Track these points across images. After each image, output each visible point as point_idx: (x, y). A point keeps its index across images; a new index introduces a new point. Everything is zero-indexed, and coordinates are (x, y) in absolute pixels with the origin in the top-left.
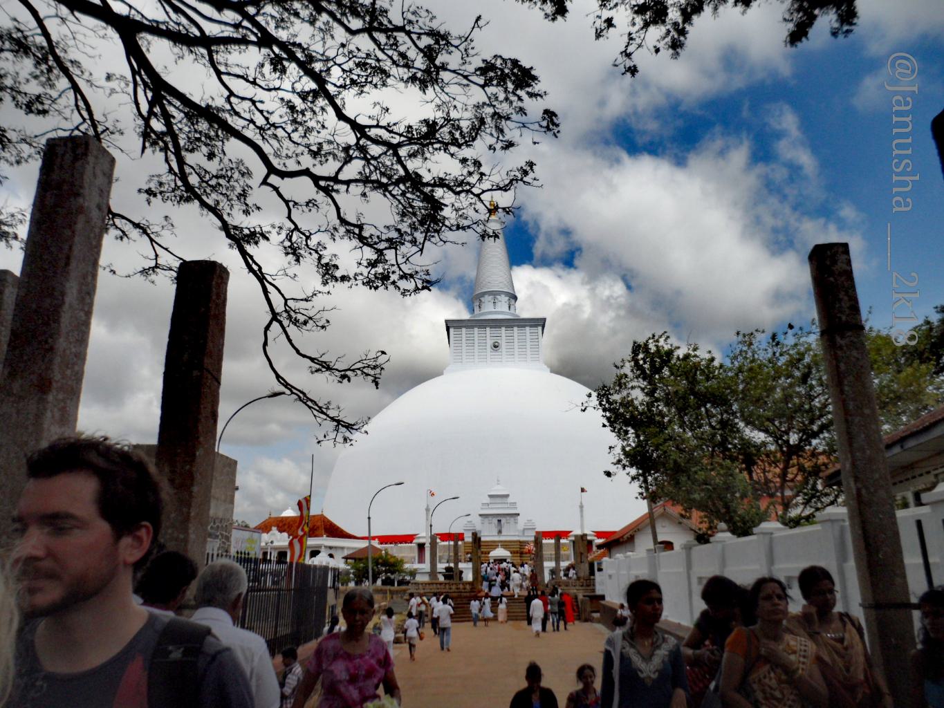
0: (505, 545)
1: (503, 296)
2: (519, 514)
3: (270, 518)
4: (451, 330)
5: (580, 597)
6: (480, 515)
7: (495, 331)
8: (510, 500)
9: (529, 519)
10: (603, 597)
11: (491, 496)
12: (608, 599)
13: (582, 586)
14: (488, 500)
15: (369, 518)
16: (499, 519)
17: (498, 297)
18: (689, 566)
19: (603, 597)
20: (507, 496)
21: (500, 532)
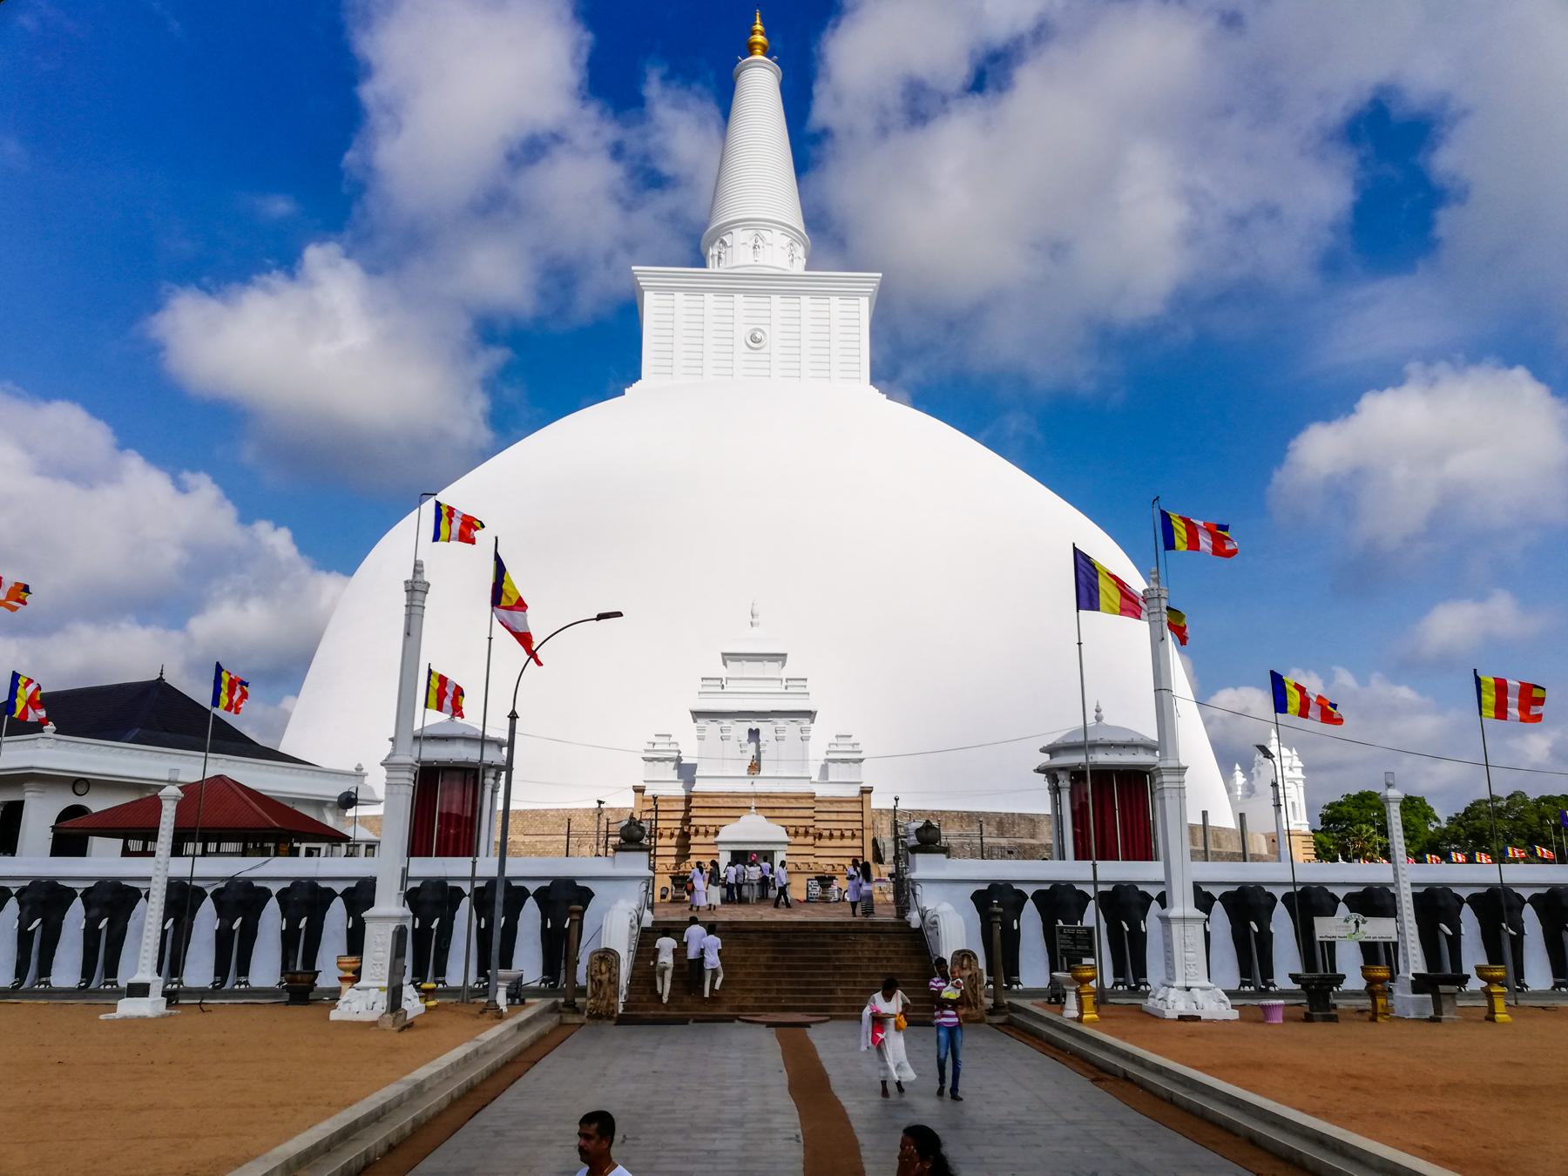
0: (770, 805)
2: (810, 714)
6: (697, 715)
7: (758, 302)
11: (728, 657)
20: (781, 658)
21: (755, 767)
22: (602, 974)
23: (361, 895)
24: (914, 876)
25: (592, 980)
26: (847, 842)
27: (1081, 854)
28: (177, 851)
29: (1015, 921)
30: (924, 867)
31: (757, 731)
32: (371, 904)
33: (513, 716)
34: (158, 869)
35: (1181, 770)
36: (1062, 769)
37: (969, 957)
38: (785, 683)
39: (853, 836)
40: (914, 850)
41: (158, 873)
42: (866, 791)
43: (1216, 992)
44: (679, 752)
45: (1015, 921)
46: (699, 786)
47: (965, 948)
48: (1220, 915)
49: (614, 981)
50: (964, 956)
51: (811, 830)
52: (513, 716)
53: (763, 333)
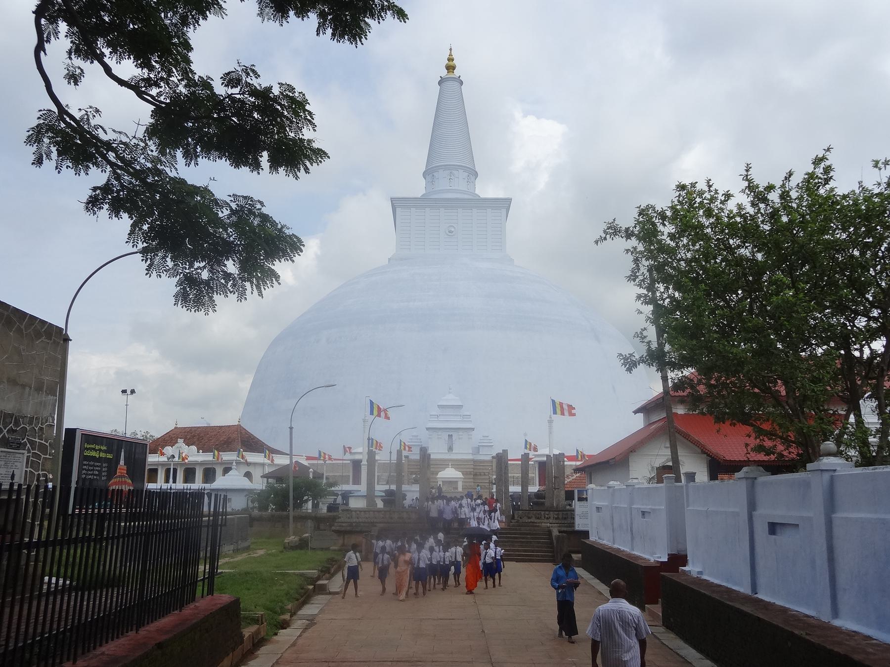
0: (458, 464)
2: (473, 429)
3: (176, 428)
4: (398, 210)
5: (555, 532)
6: (428, 429)
10: (586, 534)
12: (593, 538)
13: (556, 519)
15: (291, 428)
16: (451, 434)
17: (455, 172)
18: (752, 506)
19: (586, 534)
20: (460, 407)
21: (450, 449)
26: (483, 477)
31: (452, 435)
36: (536, 461)
44: (421, 442)
51: (472, 473)
53: (454, 228)
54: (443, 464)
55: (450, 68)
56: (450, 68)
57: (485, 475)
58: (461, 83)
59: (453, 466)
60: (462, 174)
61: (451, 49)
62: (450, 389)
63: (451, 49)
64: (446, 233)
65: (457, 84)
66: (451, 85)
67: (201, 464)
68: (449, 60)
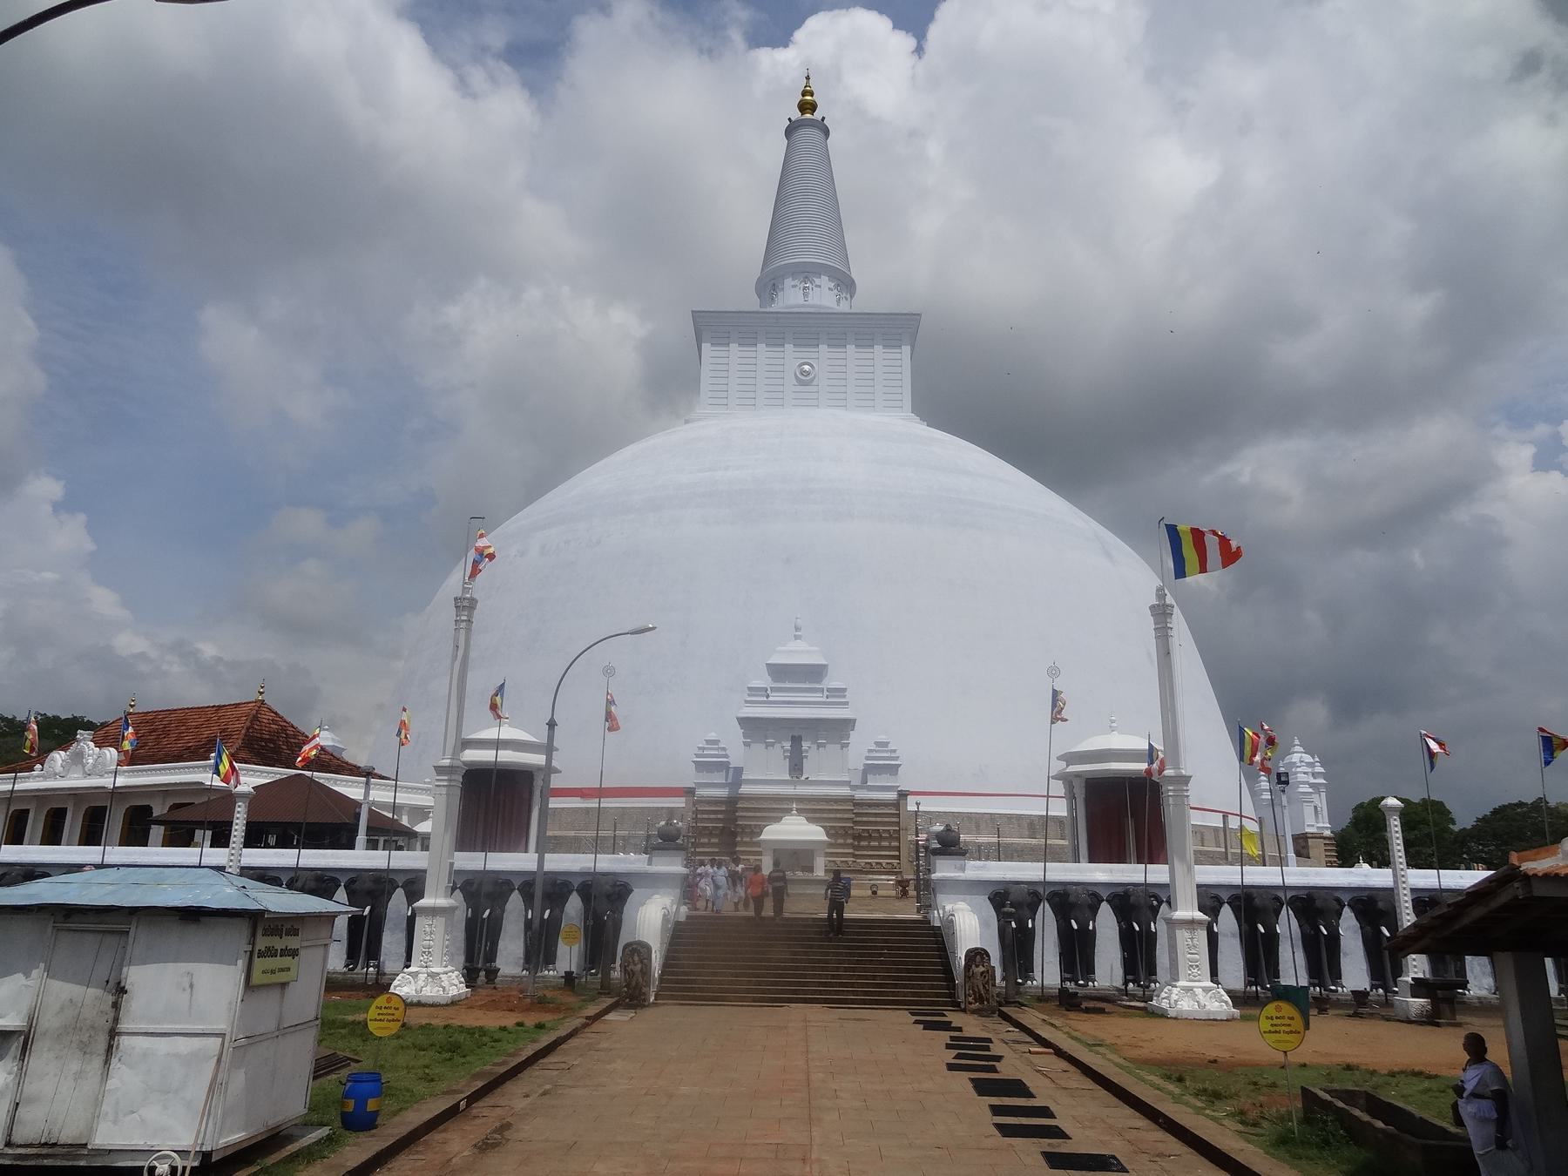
0: (814, 809)
1: (825, 278)
8: (831, 682)
9: (882, 738)
14: (764, 681)
22: (635, 965)
23: (414, 885)
24: (934, 876)
25: (626, 970)
26: (885, 844)
27: (1093, 859)
28: (249, 843)
29: (1030, 921)
30: (945, 870)
32: (422, 897)
33: (552, 725)
34: (231, 861)
35: (1186, 780)
36: (1077, 775)
37: (982, 955)
38: (826, 693)
39: (891, 838)
40: (936, 852)
41: (231, 864)
42: (903, 795)
43: (1219, 993)
44: (726, 756)
45: (1030, 921)
46: (745, 789)
47: (979, 946)
48: (1227, 920)
49: (646, 970)
50: (977, 955)
52: (552, 725)
54: (775, 807)
55: (807, 107)
56: (807, 107)
57: (881, 838)
58: (826, 132)
59: (800, 811)
60: (824, 281)
61: (808, 78)
62: (797, 629)
63: (808, 78)
64: (795, 374)
65: (815, 134)
66: (808, 135)
67: (117, 793)
68: (804, 94)
